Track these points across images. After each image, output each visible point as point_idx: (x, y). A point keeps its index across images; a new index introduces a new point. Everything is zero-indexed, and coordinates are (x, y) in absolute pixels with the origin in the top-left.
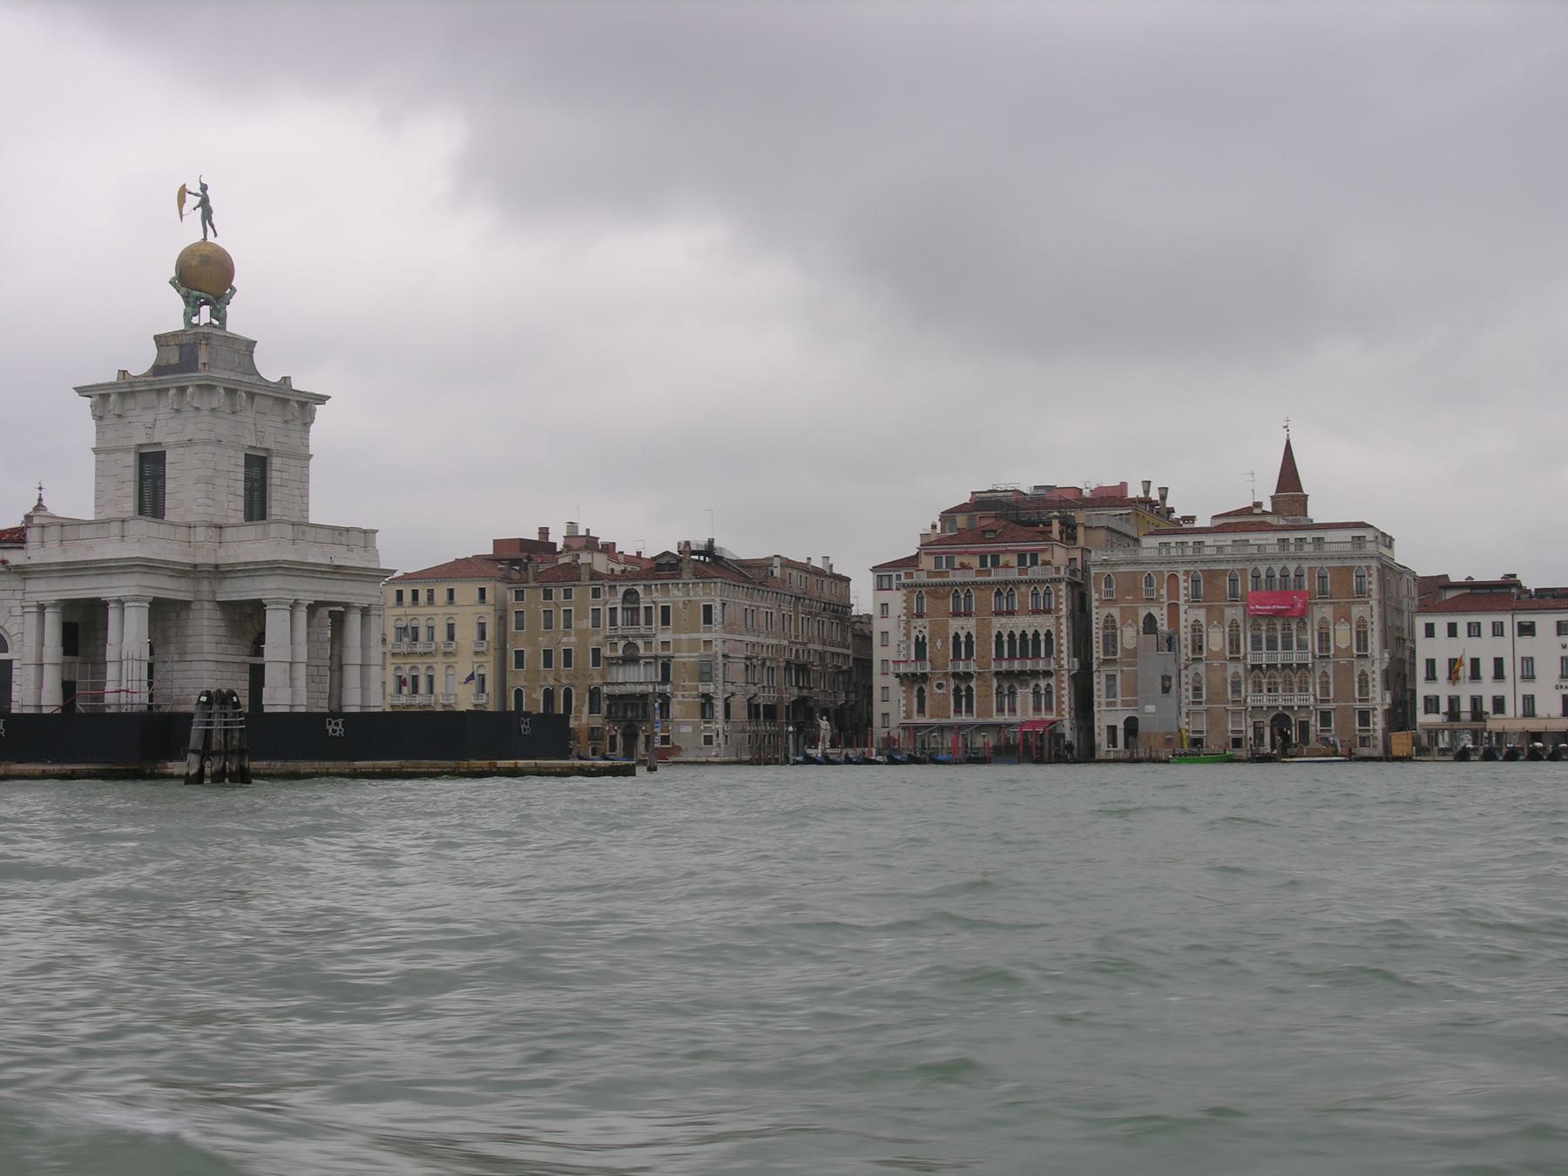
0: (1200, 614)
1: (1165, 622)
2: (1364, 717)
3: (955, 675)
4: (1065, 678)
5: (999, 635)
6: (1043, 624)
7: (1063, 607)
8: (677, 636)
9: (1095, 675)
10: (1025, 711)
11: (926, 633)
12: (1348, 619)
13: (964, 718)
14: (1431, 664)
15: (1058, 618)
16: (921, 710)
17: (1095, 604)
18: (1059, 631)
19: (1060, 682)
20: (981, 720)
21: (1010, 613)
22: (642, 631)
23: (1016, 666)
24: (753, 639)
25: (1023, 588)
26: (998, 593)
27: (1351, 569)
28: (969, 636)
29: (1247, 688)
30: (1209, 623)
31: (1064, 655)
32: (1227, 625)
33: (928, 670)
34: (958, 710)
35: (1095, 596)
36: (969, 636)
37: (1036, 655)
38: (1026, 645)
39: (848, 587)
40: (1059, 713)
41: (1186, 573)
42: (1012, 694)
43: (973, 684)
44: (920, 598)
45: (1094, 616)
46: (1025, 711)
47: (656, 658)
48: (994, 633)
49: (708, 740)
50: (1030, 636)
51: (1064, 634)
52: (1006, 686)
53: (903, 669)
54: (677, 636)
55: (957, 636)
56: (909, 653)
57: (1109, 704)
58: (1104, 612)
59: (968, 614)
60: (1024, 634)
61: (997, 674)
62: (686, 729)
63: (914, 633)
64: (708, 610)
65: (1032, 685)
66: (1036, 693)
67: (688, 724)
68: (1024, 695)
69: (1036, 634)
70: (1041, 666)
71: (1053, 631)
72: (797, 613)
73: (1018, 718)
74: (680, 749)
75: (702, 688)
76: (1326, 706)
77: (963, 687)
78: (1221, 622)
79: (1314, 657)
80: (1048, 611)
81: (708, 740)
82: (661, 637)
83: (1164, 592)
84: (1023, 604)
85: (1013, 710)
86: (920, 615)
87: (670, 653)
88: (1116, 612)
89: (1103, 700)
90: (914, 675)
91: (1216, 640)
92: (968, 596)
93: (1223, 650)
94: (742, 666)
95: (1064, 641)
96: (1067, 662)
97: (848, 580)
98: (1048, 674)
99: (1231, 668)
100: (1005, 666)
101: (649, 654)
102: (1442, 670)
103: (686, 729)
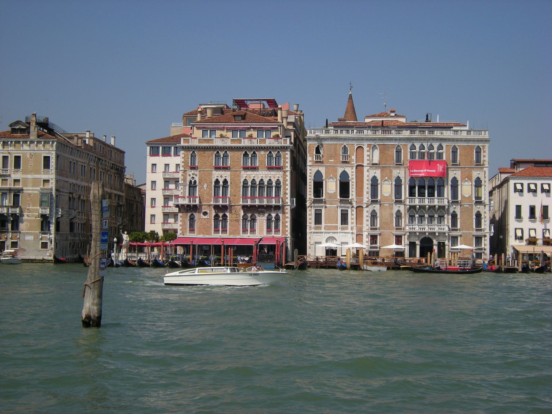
0: (378, 173)
1: (354, 177)
2: (478, 239)
3: (216, 207)
6: (275, 176)
7: (288, 165)
8: (25, 176)
9: (308, 210)
10: (261, 231)
12: (470, 179)
14: (518, 208)
15: (285, 172)
16: (192, 229)
17: (309, 163)
18: (285, 180)
19: (284, 213)
20: (231, 236)
21: (254, 169)
23: (257, 203)
24: (74, 181)
25: (262, 153)
26: (246, 155)
27: (472, 147)
28: (225, 182)
29: (405, 220)
30: (382, 177)
31: (288, 196)
32: (394, 179)
33: (197, 202)
34: (216, 230)
35: (309, 159)
36: (225, 182)
37: (269, 196)
38: (262, 187)
39: (123, 156)
40: (284, 232)
41: (369, 146)
42: (253, 220)
44: (193, 156)
45: (308, 172)
46: (261, 231)
47: (10, 190)
48: (242, 180)
49: (44, 245)
50: (266, 183)
51: (288, 182)
52: (249, 215)
53: (181, 202)
54: (25, 176)
55: (217, 182)
56: (185, 192)
57: (316, 228)
58: (315, 170)
59: (226, 168)
61: (244, 207)
62: (30, 238)
63: (189, 179)
64: (47, 159)
65: (266, 215)
66: (269, 220)
68: (261, 220)
70: (274, 203)
71: (281, 180)
72: (98, 168)
73: (257, 235)
74: (24, 250)
76: (454, 233)
77: (221, 215)
78: (390, 178)
79: (448, 202)
80: (279, 168)
81: (44, 245)
82: (14, 176)
83: (354, 157)
84: (261, 162)
85: (253, 230)
86: (193, 168)
88: (323, 170)
89: (313, 225)
90: (188, 206)
91: (386, 189)
92: (225, 156)
93: (391, 196)
94: (67, 198)
95: (288, 187)
96: (287, 199)
97: (123, 153)
98: (277, 208)
99: (396, 208)
100: (249, 203)
102: (525, 213)
103: (30, 238)
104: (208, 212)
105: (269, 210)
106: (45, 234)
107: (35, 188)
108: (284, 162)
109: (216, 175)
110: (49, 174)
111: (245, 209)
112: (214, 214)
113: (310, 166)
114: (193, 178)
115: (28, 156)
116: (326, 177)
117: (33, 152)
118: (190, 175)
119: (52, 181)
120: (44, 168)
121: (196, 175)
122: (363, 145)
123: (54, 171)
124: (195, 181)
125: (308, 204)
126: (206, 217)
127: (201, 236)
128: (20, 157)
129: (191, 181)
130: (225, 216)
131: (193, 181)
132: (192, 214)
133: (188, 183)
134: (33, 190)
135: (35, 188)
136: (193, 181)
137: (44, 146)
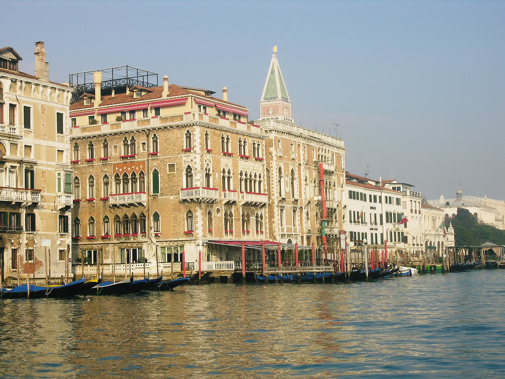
4: (267, 210)
7: (264, 158)
10: (253, 233)
17: (275, 158)
22: (7, 131)
38: (249, 182)
46: (253, 233)
47: (21, 162)
50: (253, 177)
52: (246, 214)
54: (38, 142)
67: (47, 237)
86: (209, 151)
87: (32, 157)
101: (13, 157)
107: (49, 163)
108: (263, 154)
109: (226, 163)
114: (208, 164)
115: (40, 108)
117: (44, 103)
126: (218, 215)
127: (217, 239)
128: (29, 108)
130: (231, 215)
131: (208, 168)
132: (210, 211)
134: (48, 166)
135: (49, 163)
136: (208, 168)
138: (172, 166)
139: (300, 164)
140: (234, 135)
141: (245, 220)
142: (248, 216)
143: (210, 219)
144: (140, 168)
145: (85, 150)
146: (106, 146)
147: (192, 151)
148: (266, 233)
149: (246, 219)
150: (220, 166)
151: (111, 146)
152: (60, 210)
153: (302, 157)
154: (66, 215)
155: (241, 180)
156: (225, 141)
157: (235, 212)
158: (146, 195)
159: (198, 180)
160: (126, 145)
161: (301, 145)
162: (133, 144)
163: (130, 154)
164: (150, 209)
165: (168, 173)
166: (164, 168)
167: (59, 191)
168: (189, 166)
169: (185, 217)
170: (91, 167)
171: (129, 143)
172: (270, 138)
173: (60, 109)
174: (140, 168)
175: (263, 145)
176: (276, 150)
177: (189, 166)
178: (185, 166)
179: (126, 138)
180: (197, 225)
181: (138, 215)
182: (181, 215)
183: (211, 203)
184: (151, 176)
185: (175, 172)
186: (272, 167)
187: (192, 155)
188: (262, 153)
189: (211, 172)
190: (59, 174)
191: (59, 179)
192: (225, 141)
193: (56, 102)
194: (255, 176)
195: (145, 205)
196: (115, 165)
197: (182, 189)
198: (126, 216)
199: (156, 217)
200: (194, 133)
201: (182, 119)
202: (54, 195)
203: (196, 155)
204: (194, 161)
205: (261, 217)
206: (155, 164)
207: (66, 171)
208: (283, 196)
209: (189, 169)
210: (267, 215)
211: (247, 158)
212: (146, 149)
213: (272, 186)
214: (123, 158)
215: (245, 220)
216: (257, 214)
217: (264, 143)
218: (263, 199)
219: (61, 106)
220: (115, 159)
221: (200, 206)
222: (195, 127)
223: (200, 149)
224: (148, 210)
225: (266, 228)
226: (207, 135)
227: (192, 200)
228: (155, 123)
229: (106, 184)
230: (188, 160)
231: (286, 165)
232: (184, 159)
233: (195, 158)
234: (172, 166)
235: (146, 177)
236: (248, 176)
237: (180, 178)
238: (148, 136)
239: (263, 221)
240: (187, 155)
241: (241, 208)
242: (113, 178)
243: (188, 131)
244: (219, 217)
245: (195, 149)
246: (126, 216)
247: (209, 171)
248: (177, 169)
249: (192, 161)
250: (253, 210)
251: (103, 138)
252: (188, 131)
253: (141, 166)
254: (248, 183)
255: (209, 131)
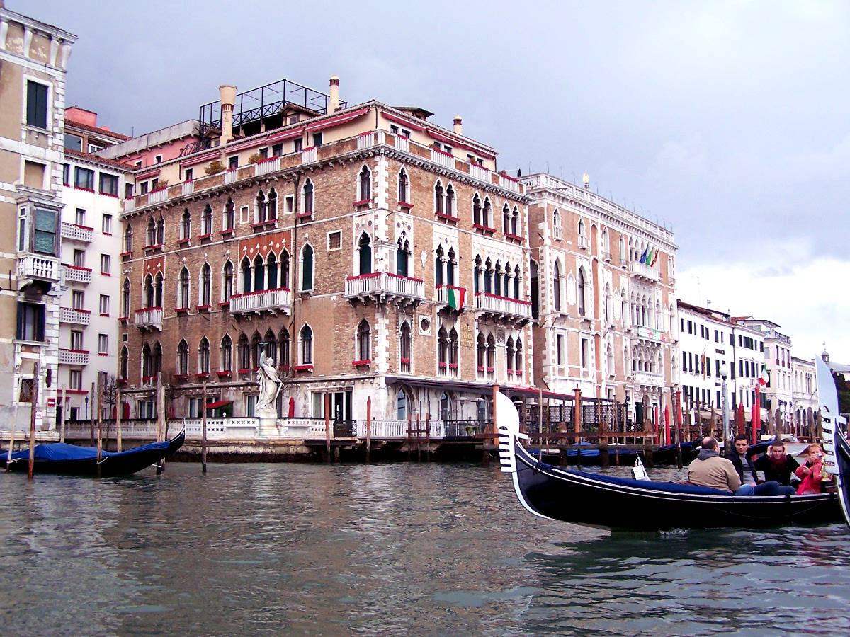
4: (530, 333)
5: (478, 261)
7: (527, 237)
10: (501, 372)
11: (410, 236)
13: (447, 377)
16: (406, 364)
17: (548, 242)
28: (451, 254)
36: (451, 254)
43: (457, 326)
46: (501, 372)
50: (503, 269)
52: (486, 336)
55: (440, 251)
60: (498, 266)
63: (397, 235)
69: (508, 268)
75: (29, 267)
77: (448, 330)
86: (406, 208)
104: (429, 319)
105: (507, 328)
106: (28, 348)
108: (523, 231)
109: (444, 235)
110: (46, 147)
111: (480, 321)
112: (438, 328)
113: (550, 247)
114: (404, 233)
116: (567, 273)
118: (399, 226)
119: (55, 173)
120: (31, 121)
121: (409, 228)
122: (597, 223)
123: (59, 140)
124: (407, 241)
125: (549, 322)
126: (426, 333)
127: (422, 377)
129: (400, 239)
130: (454, 334)
131: (404, 240)
132: (405, 324)
133: (396, 241)
136: (404, 240)
137: (33, 45)
138: (335, 237)
139: (596, 261)
140: (463, 187)
141: (485, 347)
142: (490, 340)
143: (406, 339)
144: (282, 245)
145: (199, 221)
146: (230, 212)
147: (371, 205)
148: (528, 375)
149: (486, 345)
150: (430, 240)
151: (238, 210)
152: (23, 289)
153: (600, 248)
154: (42, 303)
155: (477, 272)
156: (445, 194)
157: (463, 331)
158: (290, 295)
159: (384, 259)
160: (261, 206)
161: (598, 227)
162: (272, 204)
163: (267, 220)
164: (297, 321)
165: (329, 250)
166: (322, 242)
167: (21, 248)
168: (365, 235)
169: (356, 333)
170: (206, 250)
171: (267, 200)
172: (540, 206)
173: (37, 74)
174: (282, 245)
175: (524, 216)
176: (550, 228)
177: (365, 235)
178: (357, 235)
179: (261, 193)
180: (377, 349)
181: (276, 333)
182: (349, 331)
183: (408, 305)
184: (301, 257)
185: (341, 248)
186: (542, 258)
187: (370, 214)
188: (523, 229)
189: (411, 248)
190: (23, 211)
191: (23, 221)
192: (445, 194)
193: (27, 55)
194: (508, 268)
195: (289, 313)
196: (243, 243)
197: (351, 278)
198: (257, 336)
199: (307, 333)
200: (376, 169)
201: (355, 147)
202: (12, 256)
203: (376, 213)
204: (375, 223)
205: (519, 345)
206: (307, 235)
207: (36, 204)
208: (564, 310)
209: (365, 240)
210: (531, 342)
211: (490, 233)
212: (294, 209)
213: (543, 292)
214: (256, 228)
215: (485, 347)
216: (510, 338)
217: (526, 211)
218: (526, 312)
219: (41, 69)
220: (244, 232)
221: (384, 312)
222: (377, 159)
223: (387, 201)
224: (293, 323)
225: (528, 365)
226: (403, 176)
227: (367, 298)
228: (311, 157)
229: (229, 278)
230: (364, 223)
231: (570, 258)
232: (356, 220)
233: (376, 217)
234: (335, 237)
235: (291, 260)
236: (493, 266)
237: (349, 258)
238: (297, 184)
239: (523, 353)
240: (363, 212)
241: (476, 325)
242: (240, 266)
243: (365, 168)
244: (425, 339)
245: (376, 200)
246: (257, 336)
247: (406, 245)
248: (344, 241)
249: (370, 223)
250: (501, 330)
251: (227, 197)
252: (365, 168)
253: (284, 241)
254: (493, 279)
255: (408, 170)
